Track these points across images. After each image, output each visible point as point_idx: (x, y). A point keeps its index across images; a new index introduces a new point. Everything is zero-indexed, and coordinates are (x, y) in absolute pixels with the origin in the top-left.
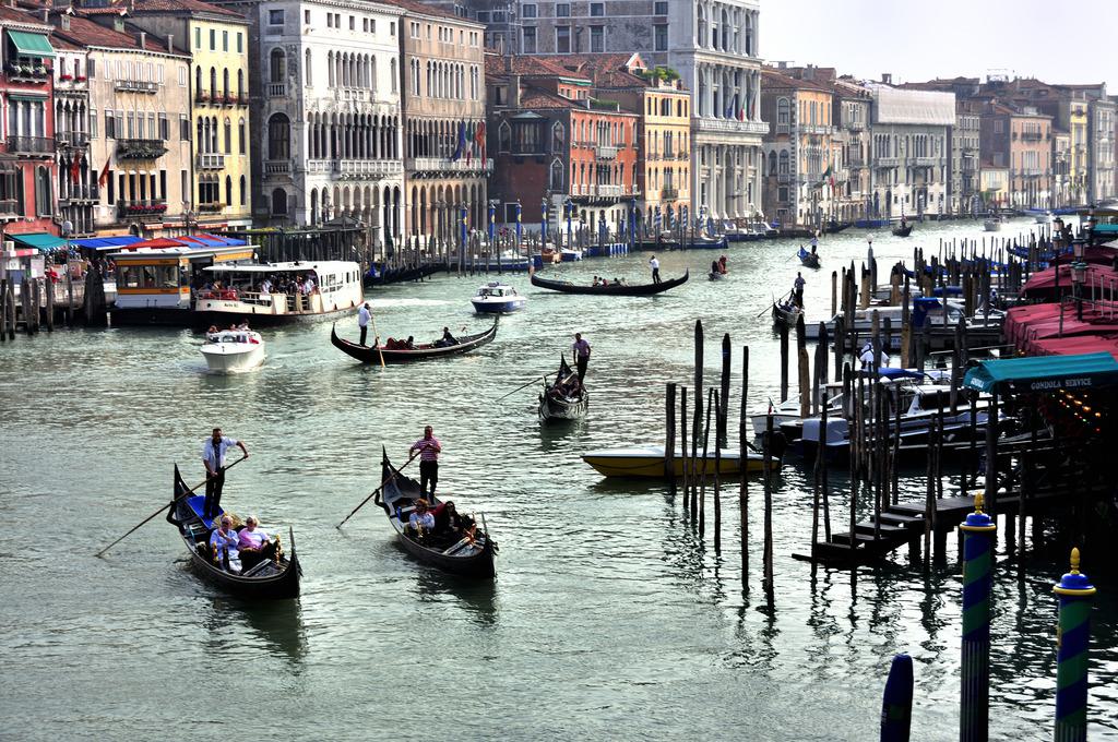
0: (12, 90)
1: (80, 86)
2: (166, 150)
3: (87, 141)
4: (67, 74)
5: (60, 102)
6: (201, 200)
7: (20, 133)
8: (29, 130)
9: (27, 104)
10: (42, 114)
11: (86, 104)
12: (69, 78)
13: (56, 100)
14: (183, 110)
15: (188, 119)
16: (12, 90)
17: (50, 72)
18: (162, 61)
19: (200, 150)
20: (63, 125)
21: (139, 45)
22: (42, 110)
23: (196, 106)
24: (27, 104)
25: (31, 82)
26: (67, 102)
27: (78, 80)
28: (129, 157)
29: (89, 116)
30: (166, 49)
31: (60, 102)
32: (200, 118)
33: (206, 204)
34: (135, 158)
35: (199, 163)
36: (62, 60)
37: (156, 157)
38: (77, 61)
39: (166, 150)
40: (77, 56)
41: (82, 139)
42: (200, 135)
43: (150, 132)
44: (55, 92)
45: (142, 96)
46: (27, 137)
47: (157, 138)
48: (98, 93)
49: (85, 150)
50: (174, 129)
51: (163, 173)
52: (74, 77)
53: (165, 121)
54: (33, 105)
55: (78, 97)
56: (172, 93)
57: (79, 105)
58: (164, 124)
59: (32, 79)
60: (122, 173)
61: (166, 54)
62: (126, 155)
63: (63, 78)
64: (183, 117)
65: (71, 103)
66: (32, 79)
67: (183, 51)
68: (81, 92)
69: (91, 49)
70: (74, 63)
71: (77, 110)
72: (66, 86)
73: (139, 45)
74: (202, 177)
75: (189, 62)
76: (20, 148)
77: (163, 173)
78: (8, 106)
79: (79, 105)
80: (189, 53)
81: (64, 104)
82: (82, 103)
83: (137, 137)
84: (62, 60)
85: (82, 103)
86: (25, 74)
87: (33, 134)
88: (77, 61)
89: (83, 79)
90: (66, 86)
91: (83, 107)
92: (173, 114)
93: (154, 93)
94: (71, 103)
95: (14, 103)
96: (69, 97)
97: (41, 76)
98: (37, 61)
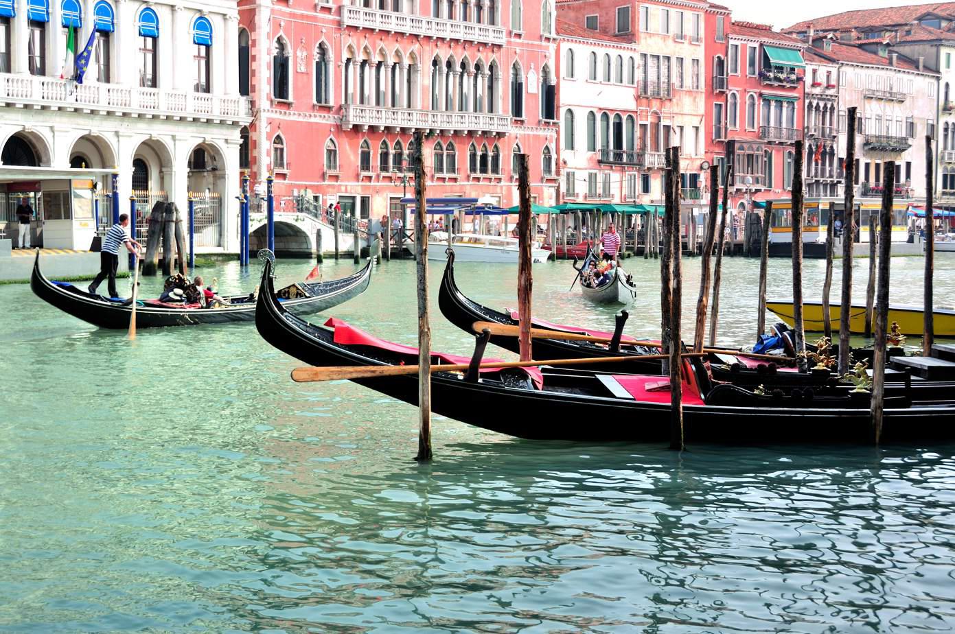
0: (766, 91)
1: (831, 92)
2: (910, 146)
3: (835, 134)
4: (819, 81)
5: (810, 103)
6: (945, 187)
7: (772, 124)
8: (781, 123)
9: (779, 103)
10: (793, 111)
11: (835, 105)
12: (819, 85)
13: (807, 101)
14: (931, 116)
15: (935, 123)
16: (766, 91)
17: (799, 79)
18: (911, 77)
19: (945, 148)
20: (813, 120)
21: (891, 63)
22: (793, 108)
23: (943, 114)
24: (779, 103)
25: (784, 86)
26: (818, 104)
27: (829, 87)
28: (873, 149)
29: (839, 115)
30: (917, 68)
31: (810, 103)
32: (947, 123)
33: (948, 190)
34: (882, 150)
35: (943, 158)
36: (815, 71)
37: (904, 150)
38: (829, 73)
39: (910, 146)
40: (830, 69)
41: (830, 132)
42: (946, 136)
43: (897, 131)
44: (806, 95)
45: (891, 104)
46: (779, 128)
47: (904, 135)
48: (847, 98)
49: (833, 141)
50: (921, 132)
51: (908, 164)
52: (825, 84)
53: (912, 124)
54: (785, 105)
55: (829, 100)
56: (920, 102)
57: (829, 106)
58: (911, 126)
59: (784, 84)
60: (868, 161)
61: (916, 72)
62: (870, 147)
63: (815, 85)
64: (930, 122)
65: (822, 104)
66: (784, 84)
67: (933, 70)
68: (831, 96)
69: (842, 64)
70: (825, 74)
71: (826, 111)
72: (817, 91)
73: (891, 63)
74: (946, 169)
75: (938, 79)
76: (772, 135)
77: (908, 164)
78: (762, 103)
79: (829, 106)
80: (938, 72)
81: (814, 105)
82: (832, 105)
83: (884, 133)
84: (815, 71)
85: (832, 105)
86: (777, 79)
87: (784, 125)
88: (829, 73)
89: (833, 87)
90: (817, 91)
91: (832, 108)
92: (919, 119)
93: (903, 102)
94: (822, 104)
95: (767, 101)
96: (819, 99)
97: (793, 82)
98: (792, 70)
